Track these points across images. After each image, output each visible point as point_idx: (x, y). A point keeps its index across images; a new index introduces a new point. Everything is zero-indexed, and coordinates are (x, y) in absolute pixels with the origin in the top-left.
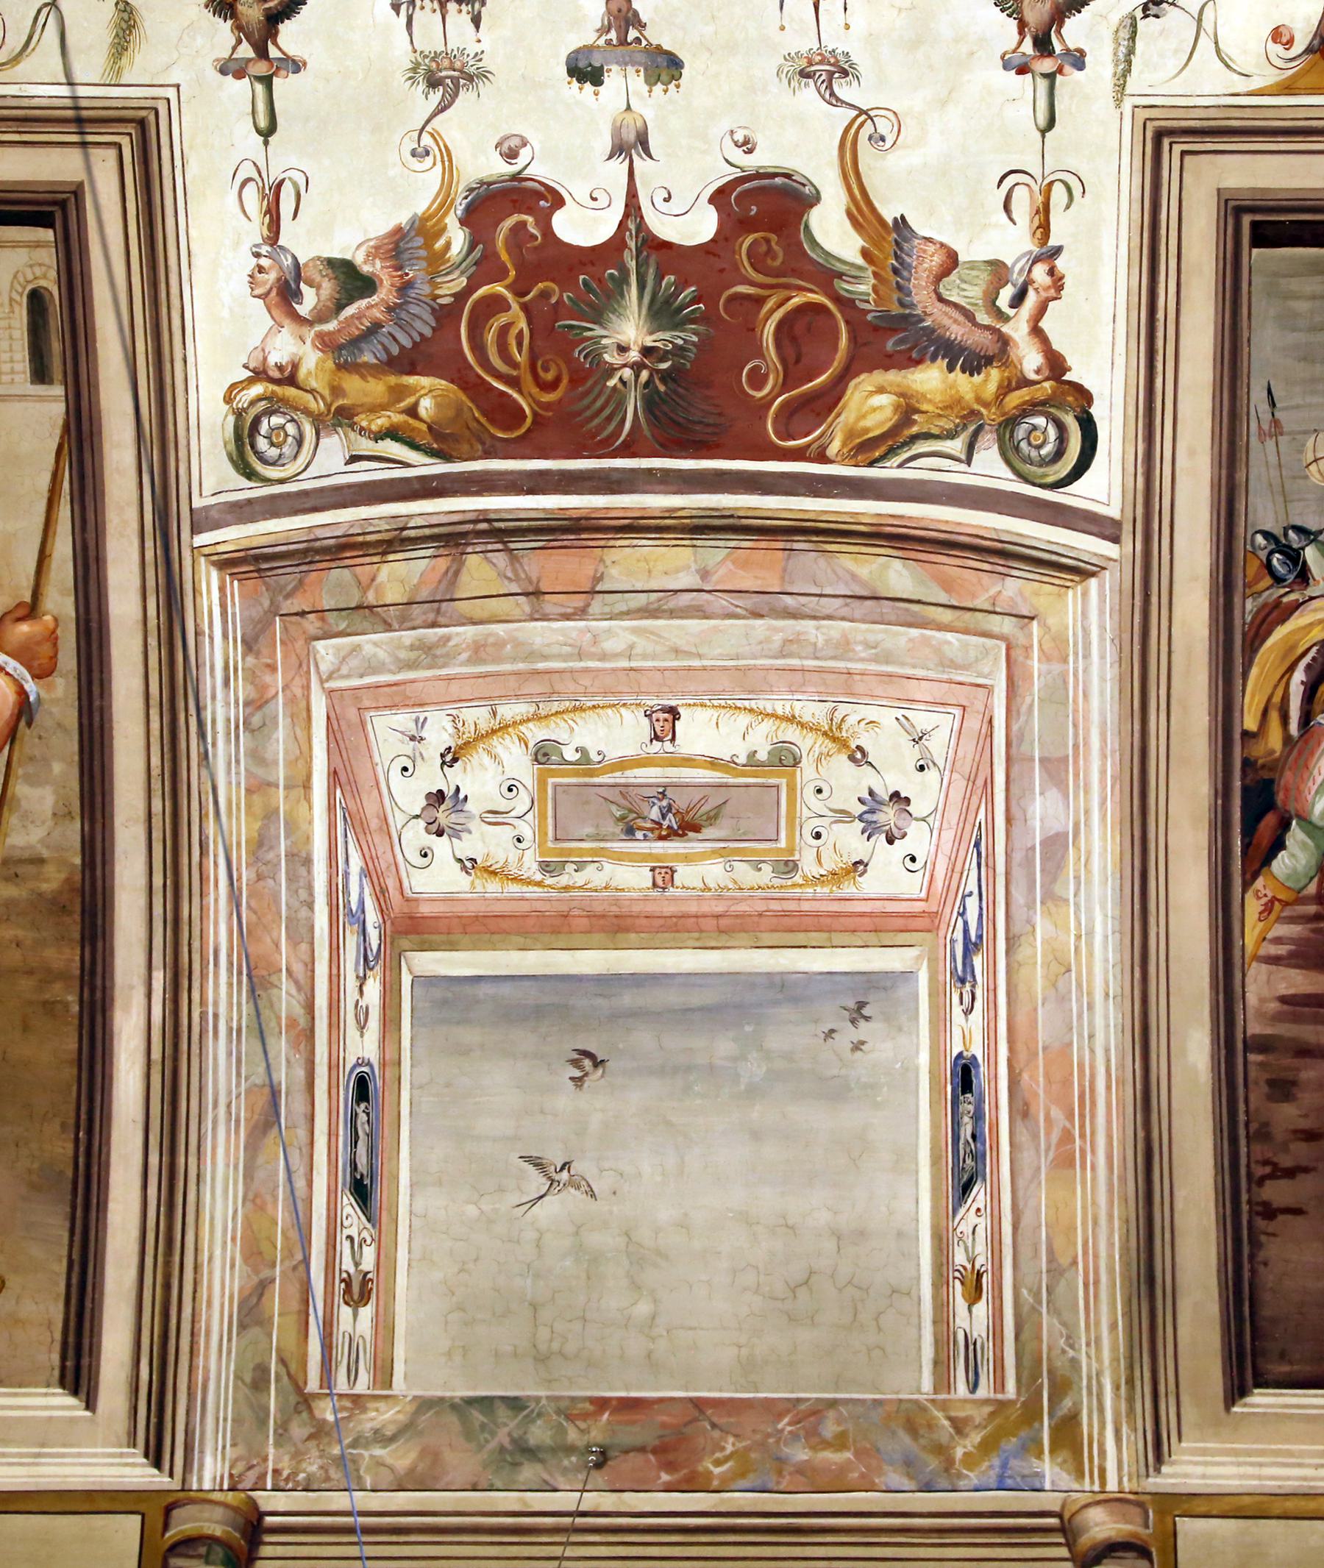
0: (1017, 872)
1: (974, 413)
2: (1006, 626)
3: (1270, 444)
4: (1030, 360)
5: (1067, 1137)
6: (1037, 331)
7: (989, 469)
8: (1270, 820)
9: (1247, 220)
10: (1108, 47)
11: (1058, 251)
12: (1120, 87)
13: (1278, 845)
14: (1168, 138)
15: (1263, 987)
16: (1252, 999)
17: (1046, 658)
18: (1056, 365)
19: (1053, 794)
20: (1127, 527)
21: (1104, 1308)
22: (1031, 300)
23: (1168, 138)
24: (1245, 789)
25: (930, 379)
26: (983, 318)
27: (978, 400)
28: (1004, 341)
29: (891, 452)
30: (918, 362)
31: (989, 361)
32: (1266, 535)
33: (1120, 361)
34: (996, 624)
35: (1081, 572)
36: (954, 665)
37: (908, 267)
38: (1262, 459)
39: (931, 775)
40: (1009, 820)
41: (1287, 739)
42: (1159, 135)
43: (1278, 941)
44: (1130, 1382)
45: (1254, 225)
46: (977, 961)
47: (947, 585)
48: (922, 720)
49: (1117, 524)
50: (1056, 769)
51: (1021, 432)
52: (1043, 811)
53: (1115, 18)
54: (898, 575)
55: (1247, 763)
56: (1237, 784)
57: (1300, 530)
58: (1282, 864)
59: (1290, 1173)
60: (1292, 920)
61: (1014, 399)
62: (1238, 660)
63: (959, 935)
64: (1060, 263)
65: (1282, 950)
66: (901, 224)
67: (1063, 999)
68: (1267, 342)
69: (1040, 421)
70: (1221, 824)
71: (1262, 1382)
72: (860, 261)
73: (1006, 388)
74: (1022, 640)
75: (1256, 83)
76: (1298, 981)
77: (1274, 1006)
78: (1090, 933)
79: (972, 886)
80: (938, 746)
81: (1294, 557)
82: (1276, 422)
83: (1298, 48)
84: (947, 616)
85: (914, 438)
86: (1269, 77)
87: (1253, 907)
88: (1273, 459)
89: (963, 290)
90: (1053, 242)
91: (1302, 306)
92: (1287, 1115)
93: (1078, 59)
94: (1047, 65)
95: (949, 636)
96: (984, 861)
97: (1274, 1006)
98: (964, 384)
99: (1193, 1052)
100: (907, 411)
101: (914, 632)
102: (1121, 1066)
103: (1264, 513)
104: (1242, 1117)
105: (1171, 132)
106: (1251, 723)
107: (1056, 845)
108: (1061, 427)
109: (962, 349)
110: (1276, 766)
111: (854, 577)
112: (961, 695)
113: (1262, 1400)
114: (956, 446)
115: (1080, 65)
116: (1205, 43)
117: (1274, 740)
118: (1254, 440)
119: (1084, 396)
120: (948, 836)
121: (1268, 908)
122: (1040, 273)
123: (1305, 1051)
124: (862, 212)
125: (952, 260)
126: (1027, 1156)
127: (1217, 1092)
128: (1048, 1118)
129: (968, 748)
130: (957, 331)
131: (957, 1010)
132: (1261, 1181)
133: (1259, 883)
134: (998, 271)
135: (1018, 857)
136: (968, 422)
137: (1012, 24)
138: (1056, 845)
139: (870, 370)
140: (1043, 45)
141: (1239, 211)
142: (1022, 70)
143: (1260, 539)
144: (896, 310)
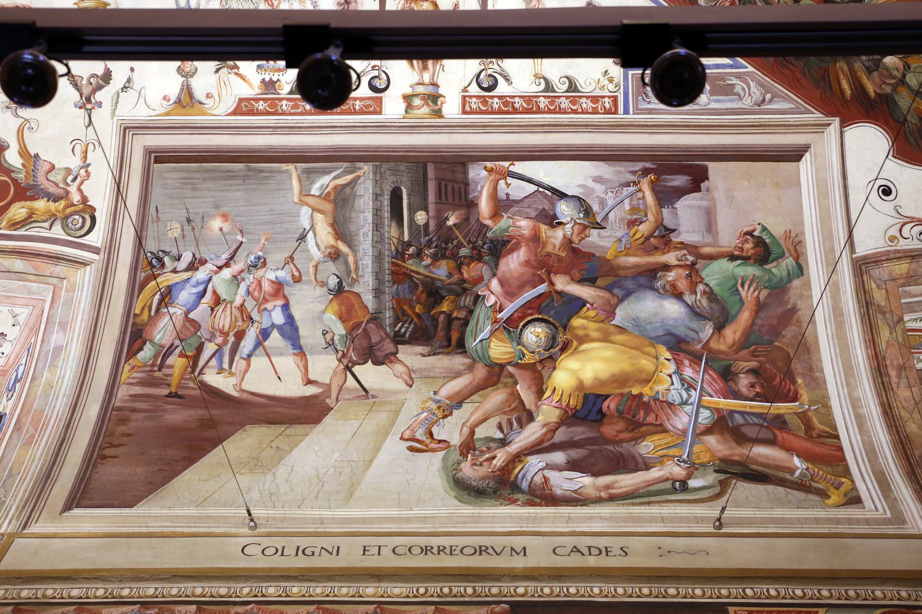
0: (41, 357)
1: (54, 215)
2: (55, 281)
3: (155, 224)
4: (76, 198)
5: (33, 436)
6: (79, 189)
7: (57, 231)
8: (139, 341)
9: (153, 155)
10: (110, 101)
11: (89, 165)
12: (113, 114)
13: (141, 349)
14: (128, 130)
15: (123, 392)
16: (119, 396)
17: (67, 291)
18: (84, 200)
19: (61, 333)
20: (103, 250)
21: (24, 485)
22: (79, 180)
23: (128, 130)
24: (131, 332)
25: (41, 205)
26: (61, 185)
27: (57, 210)
28: (68, 193)
29: (23, 226)
30: (36, 199)
31: (62, 198)
32: (151, 253)
33: (107, 199)
34: (51, 280)
35: (84, 264)
36: (34, 293)
37: (38, 170)
38: (151, 230)
39: (17, 328)
40: (42, 342)
41: (150, 316)
42: (125, 129)
43: (134, 378)
44: (24, 507)
45: (155, 157)
46: (18, 385)
47: (35, 268)
48: (17, 310)
49: (99, 249)
50: (63, 326)
51: (70, 220)
52: (56, 338)
53: (113, 92)
54: (18, 264)
55: (134, 324)
56: (129, 330)
57: (163, 251)
58: (141, 355)
59: (117, 446)
60: (141, 372)
61: (69, 210)
62: (136, 295)
63: (13, 377)
64: (90, 169)
65: (135, 381)
66: (37, 156)
67: (47, 396)
68: (157, 193)
69: (77, 217)
70: (121, 342)
71: (78, 506)
72: (21, 167)
73: (67, 207)
74: (60, 285)
75: (157, 113)
76: (138, 390)
77: (128, 398)
78: (64, 377)
79: (23, 362)
80: (21, 319)
81: (160, 260)
82: (158, 217)
83: (172, 102)
84: (34, 278)
85: (32, 222)
86: (163, 111)
87: (127, 367)
88: (156, 229)
89: (56, 177)
90: (88, 162)
91: (170, 182)
92: (122, 429)
93: (100, 105)
94: (89, 106)
95: (34, 284)
96: (30, 354)
97: (128, 398)
98: (52, 206)
99: (92, 411)
100: (31, 214)
101: (21, 283)
102: (62, 415)
103: (151, 246)
104: (104, 430)
105: (129, 128)
106: (137, 311)
107: (58, 350)
108: (84, 219)
109: (53, 195)
110: (145, 325)
111: (2, 265)
112: (34, 303)
113: (76, 512)
114: (47, 225)
115: (100, 106)
116: (142, 100)
117: (145, 316)
118: (150, 223)
119: (93, 209)
120: (19, 346)
121: (133, 368)
122: (83, 172)
123: (134, 410)
124: (24, 152)
125: (53, 167)
126: (14, 442)
127: (96, 424)
128: (27, 430)
129: (33, 319)
130: (52, 189)
131: (5, 399)
132: (104, 449)
133: (131, 361)
134: (68, 171)
135: (43, 353)
136: (52, 218)
137: (78, 94)
138: (58, 350)
139: (20, 201)
140: (88, 100)
141: (151, 152)
142: (81, 108)
143: (149, 254)
144: (32, 183)
